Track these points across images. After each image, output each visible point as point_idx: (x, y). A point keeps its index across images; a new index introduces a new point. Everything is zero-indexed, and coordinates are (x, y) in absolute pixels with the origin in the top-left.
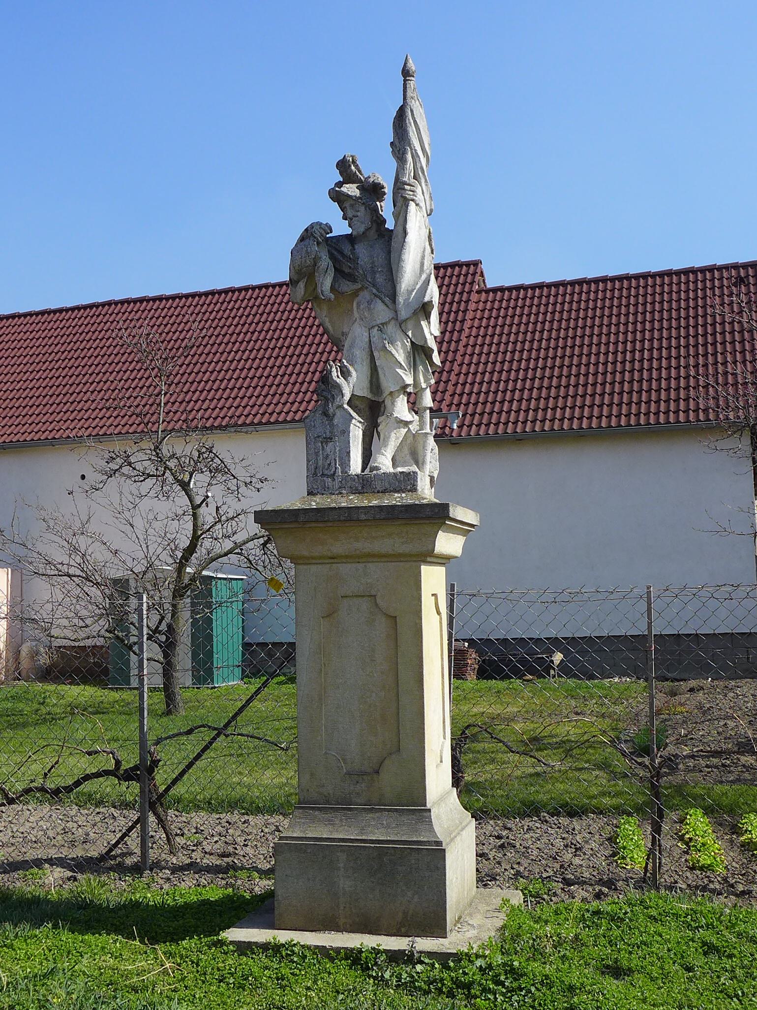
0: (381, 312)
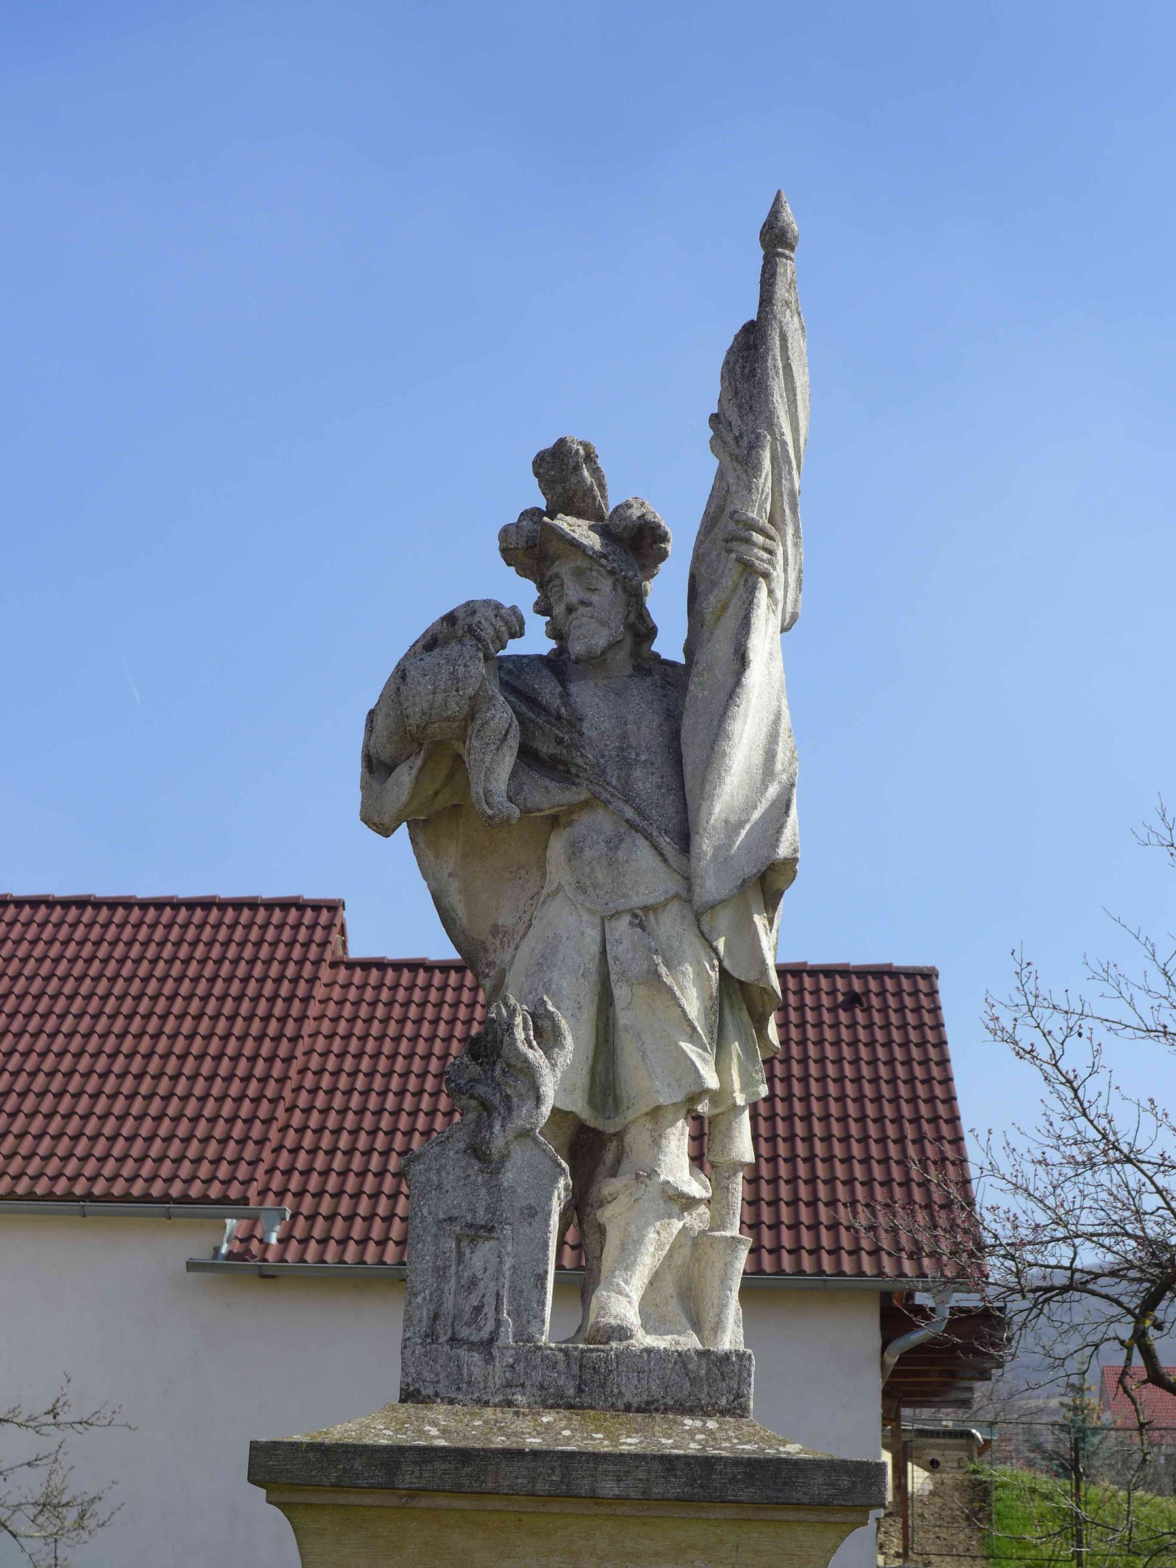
0: (646, 873)
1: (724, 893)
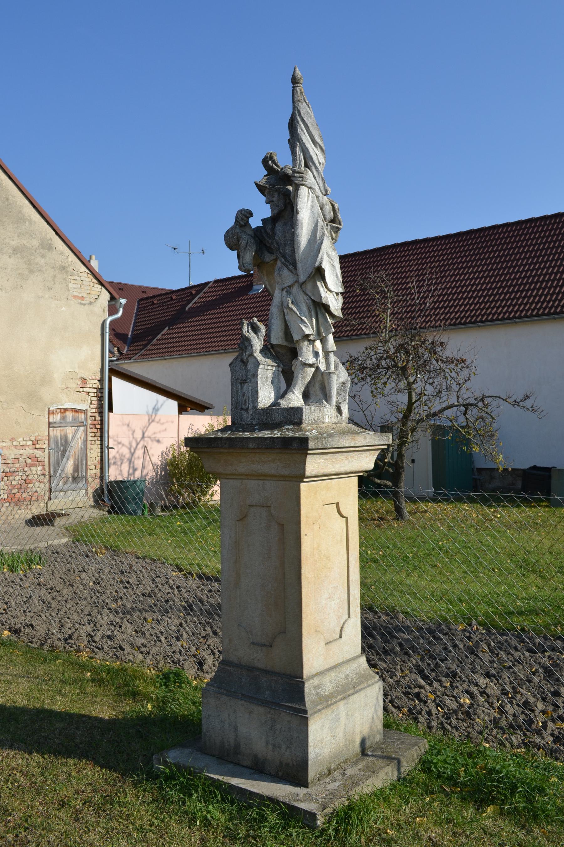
1: (305, 279)
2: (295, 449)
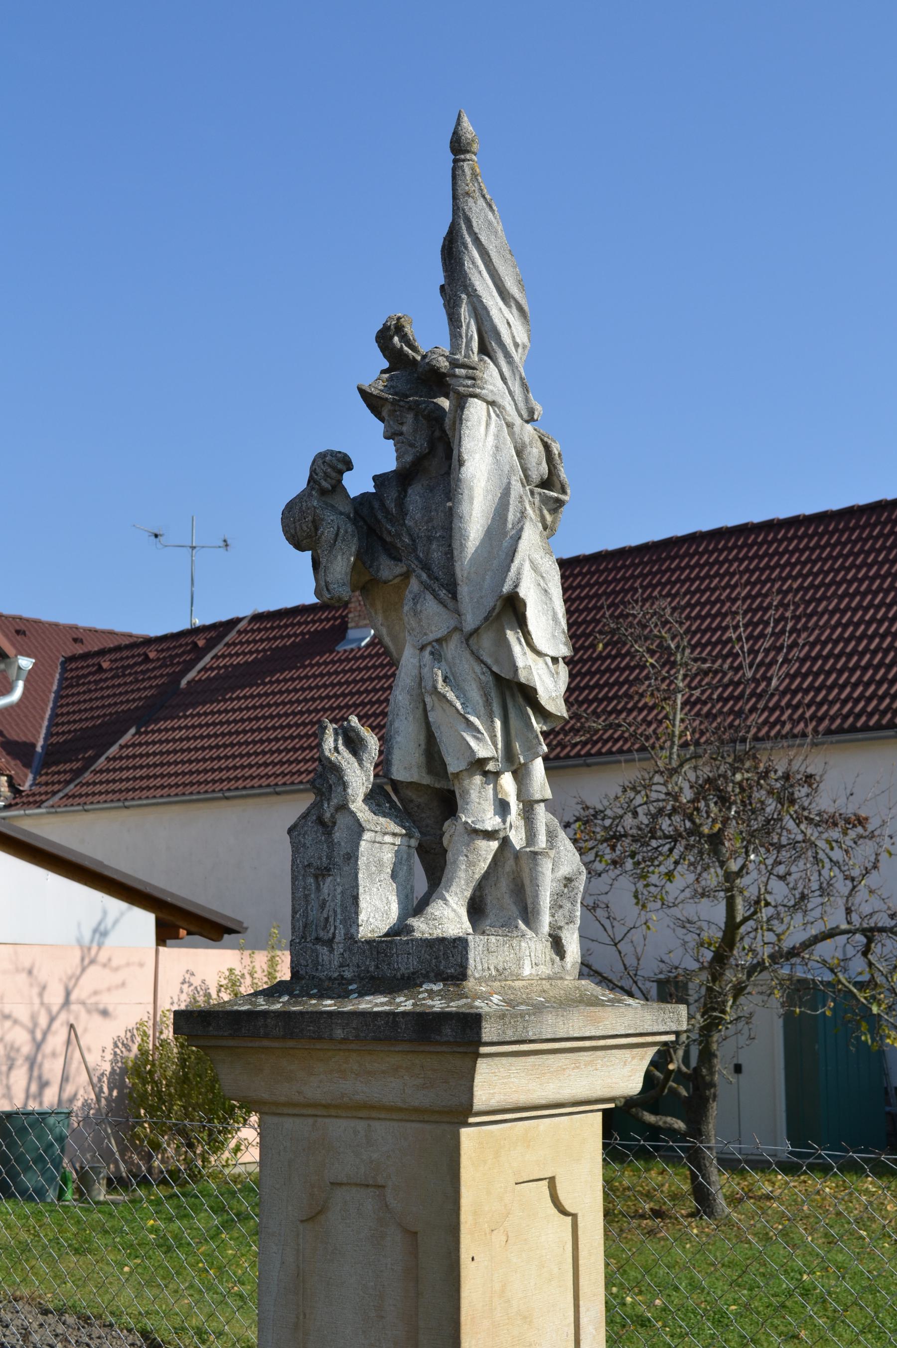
1: (478, 623)
2: (447, 1043)
